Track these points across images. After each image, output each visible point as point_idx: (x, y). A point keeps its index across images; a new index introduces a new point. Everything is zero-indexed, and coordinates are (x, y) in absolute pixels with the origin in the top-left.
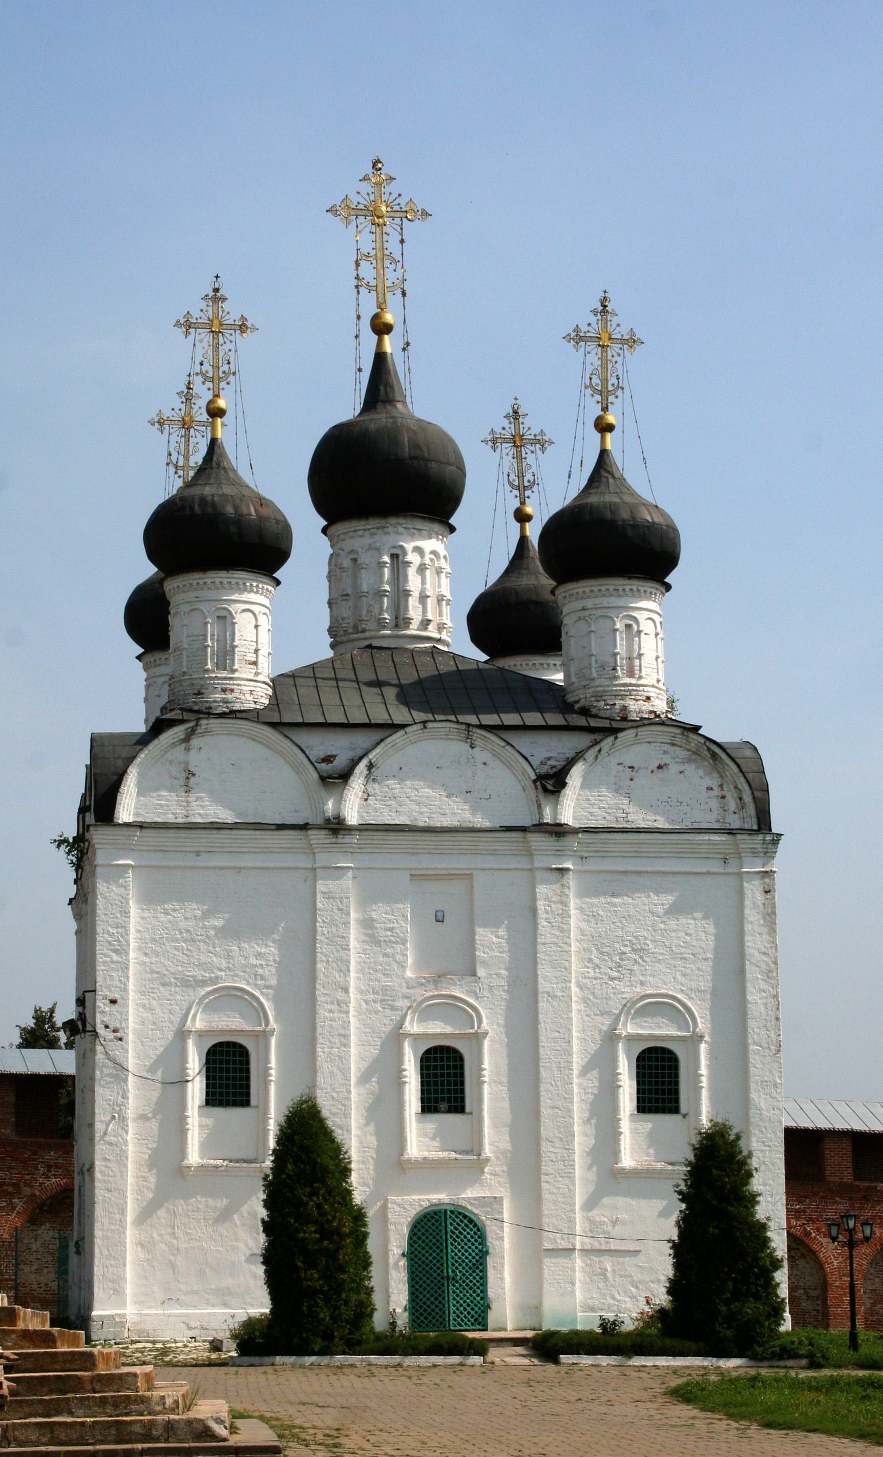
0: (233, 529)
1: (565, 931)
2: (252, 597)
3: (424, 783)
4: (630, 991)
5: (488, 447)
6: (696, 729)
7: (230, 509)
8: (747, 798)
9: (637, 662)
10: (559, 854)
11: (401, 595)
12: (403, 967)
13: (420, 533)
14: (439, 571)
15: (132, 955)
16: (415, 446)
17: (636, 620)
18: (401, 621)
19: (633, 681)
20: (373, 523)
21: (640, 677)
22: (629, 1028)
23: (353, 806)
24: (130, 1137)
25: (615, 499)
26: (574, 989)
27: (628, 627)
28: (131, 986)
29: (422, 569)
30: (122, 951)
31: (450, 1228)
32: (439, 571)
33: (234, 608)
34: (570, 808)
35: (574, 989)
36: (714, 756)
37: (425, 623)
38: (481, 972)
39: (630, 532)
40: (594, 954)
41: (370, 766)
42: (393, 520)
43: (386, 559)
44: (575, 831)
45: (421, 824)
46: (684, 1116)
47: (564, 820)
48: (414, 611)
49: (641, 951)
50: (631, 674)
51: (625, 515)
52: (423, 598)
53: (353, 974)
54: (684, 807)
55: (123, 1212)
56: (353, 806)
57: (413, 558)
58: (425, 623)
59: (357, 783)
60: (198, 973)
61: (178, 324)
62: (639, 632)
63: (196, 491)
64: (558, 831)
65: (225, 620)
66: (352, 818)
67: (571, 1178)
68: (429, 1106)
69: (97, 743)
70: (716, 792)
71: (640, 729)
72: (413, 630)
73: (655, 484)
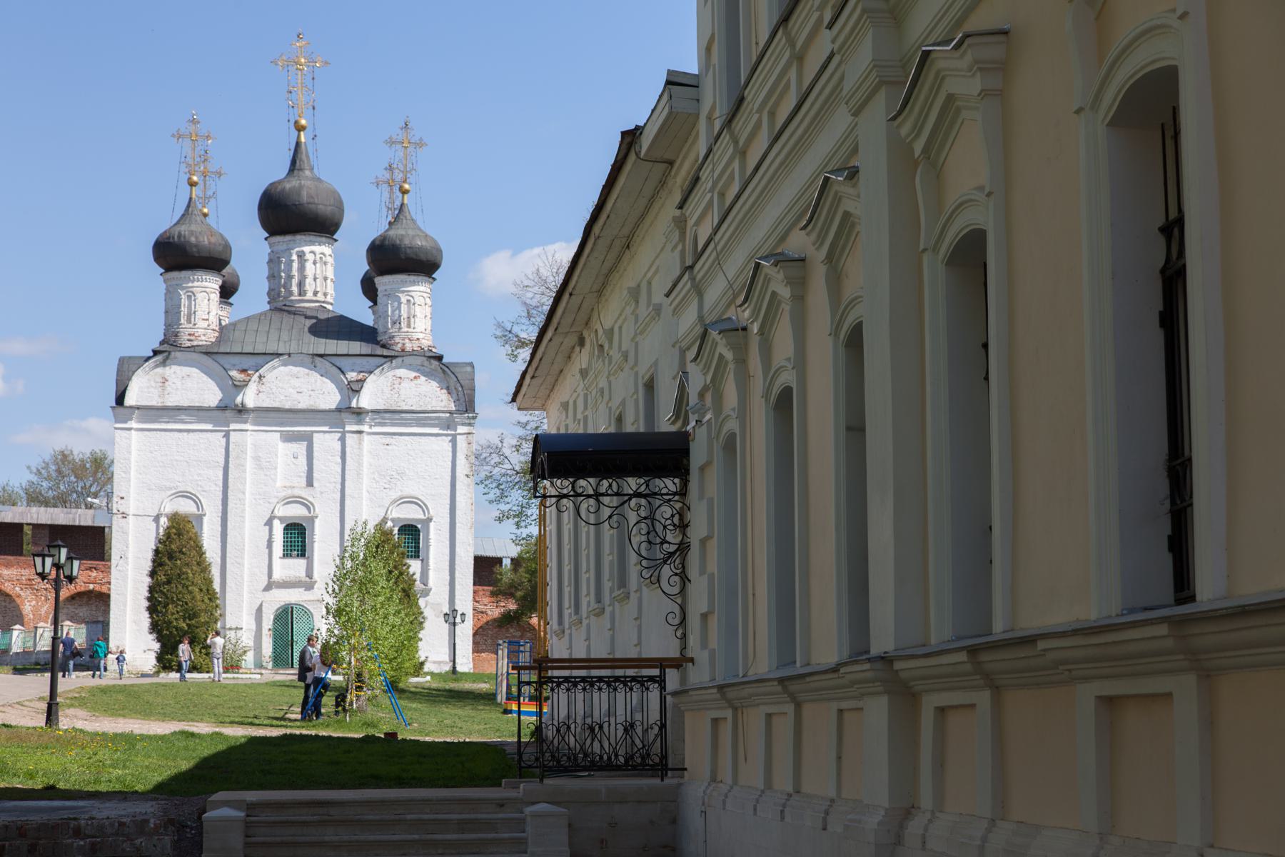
1: (360, 464)
3: (293, 384)
4: (395, 495)
5: (374, 187)
6: (440, 358)
7: (193, 239)
8: (461, 394)
10: (360, 422)
12: (275, 481)
13: (312, 243)
14: (325, 263)
15: (132, 473)
16: (310, 196)
18: (302, 292)
20: (288, 238)
23: (250, 397)
24: (130, 567)
25: (403, 232)
26: (365, 494)
28: (132, 490)
30: (127, 472)
32: (325, 263)
34: (366, 400)
35: (365, 494)
36: (444, 372)
37: (315, 293)
38: (315, 484)
40: (376, 476)
41: (260, 377)
42: (298, 237)
43: (295, 257)
44: (367, 412)
47: (361, 405)
48: (309, 286)
49: (401, 474)
50: (409, 326)
51: (407, 242)
52: (315, 279)
55: (125, 605)
57: (310, 257)
58: (315, 293)
60: (168, 484)
61: (173, 136)
63: (177, 229)
66: (250, 403)
68: (287, 555)
69: (122, 361)
72: (309, 296)
73: (429, 225)
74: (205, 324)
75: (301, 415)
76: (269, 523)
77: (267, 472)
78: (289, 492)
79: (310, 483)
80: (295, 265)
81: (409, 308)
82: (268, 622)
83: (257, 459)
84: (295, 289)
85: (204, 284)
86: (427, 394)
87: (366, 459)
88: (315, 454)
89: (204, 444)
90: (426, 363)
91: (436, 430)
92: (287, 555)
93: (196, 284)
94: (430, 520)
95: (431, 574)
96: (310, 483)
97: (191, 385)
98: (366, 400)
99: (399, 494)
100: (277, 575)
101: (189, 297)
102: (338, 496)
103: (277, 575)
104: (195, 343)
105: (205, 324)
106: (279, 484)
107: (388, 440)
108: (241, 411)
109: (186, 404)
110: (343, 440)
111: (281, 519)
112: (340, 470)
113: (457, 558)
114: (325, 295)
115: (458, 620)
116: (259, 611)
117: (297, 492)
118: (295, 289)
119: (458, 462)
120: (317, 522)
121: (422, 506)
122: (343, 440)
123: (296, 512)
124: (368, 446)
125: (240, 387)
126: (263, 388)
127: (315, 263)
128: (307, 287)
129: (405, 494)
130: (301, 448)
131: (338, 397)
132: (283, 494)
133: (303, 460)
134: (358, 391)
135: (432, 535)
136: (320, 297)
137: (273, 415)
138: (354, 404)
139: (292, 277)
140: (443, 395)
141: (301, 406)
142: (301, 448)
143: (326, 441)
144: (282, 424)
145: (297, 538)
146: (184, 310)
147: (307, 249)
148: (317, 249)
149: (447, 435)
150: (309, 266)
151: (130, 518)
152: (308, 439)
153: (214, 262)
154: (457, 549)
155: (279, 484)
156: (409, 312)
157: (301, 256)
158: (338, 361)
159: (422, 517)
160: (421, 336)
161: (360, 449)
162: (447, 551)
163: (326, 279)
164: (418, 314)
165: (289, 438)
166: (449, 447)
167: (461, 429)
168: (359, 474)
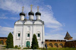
4: (37, 31)
22: (37, 33)
34: (35, 23)
49: (38, 29)
56: (25, 23)
64: (34, 24)
65: (22, 17)
68: (28, 36)
76: (26, 34)
77: (26, 30)
82: (26, 43)
83: (25, 28)
86: (40, 23)
87: (35, 28)
89: (21, 27)
92: (28, 36)
97: (21, 23)
98: (35, 23)
100: (27, 38)
103: (27, 38)
108: (24, 24)
116: (25, 42)
121: (40, 32)
123: (29, 33)
125: (24, 22)
130: (29, 28)
133: (29, 28)
142: (29, 28)
143: (31, 27)
145: (29, 35)
153: (24, 15)
165: (28, 27)
166: (42, 27)
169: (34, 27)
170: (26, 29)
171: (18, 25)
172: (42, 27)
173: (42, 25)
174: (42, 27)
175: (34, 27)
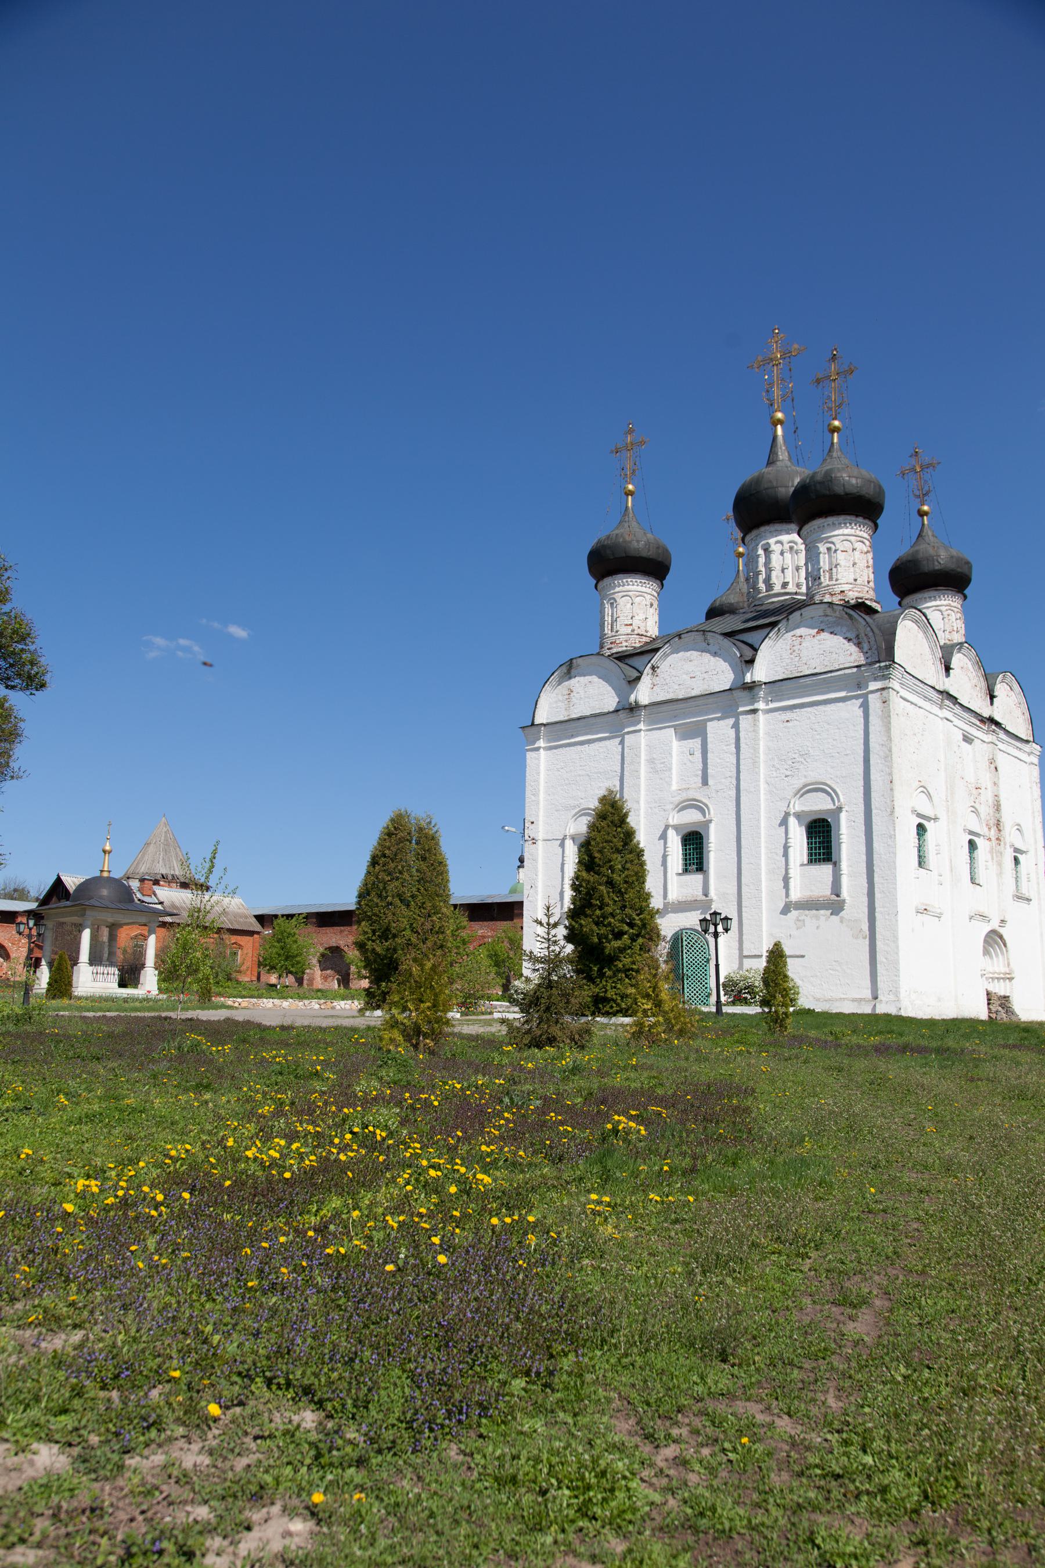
0: (608, 552)
1: (756, 750)
2: (630, 588)
4: (798, 783)
9: (834, 570)
11: (769, 570)
12: (670, 784)
13: (779, 533)
17: (833, 543)
18: (769, 586)
19: (834, 582)
21: (837, 580)
22: (798, 806)
26: (762, 786)
27: (829, 549)
28: (541, 813)
29: (782, 553)
31: (685, 943)
33: (617, 596)
34: (761, 671)
35: (762, 786)
37: (785, 585)
39: (818, 487)
41: (653, 668)
42: (762, 529)
43: (761, 552)
45: (681, 697)
46: (835, 864)
47: (756, 679)
48: (776, 579)
53: (643, 792)
54: (834, 655)
56: (644, 693)
57: (773, 547)
58: (785, 585)
59: (646, 680)
62: (836, 551)
66: (644, 700)
67: (761, 909)
70: (855, 641)
71: (803, 611)
72: (777, 589)
74: (629, 630)
75: (691, 703)
78: (685, 796)
79: (705, 782)
80: (762, 560)
81: (830, 557)
83: (651, 761)
84: (762, 586)
85: (627, 588)
88: (710, 746)
90: (829, 611)
91: (843, 694)
93: (617, 589)
94: (840, 809)
95: (845, 881)
96: (705, 782)
97: (593, 694)
99: (803, 781)
101: (612, 604)
102: (733, 793)
104: (614, 651)
105: (629, 630)
106: (674, 787)
107: (788, 715)
109: (588, 712)
110: (736, 726)
111: (676, 828)
112: (735, 762)
113: (875, 856)
114: (798, 585)
115: (720, 928)
117: (692, 794)
118: (762, 586)
119: (871, 729)
120: (712, 827)
122: (736, 726)
123: (691, 817)
124: (764, 725)
126: (657, 680)
127: (782, 553)
128: (774, 580)
129: (809, 780)
130: (696, 743)
131: (732, 676)
132: (678, 799)
133: (698, 755)
134: (751, 662)
135: (844, 829)
136: (791, 588)
137: (664, 708)
138: (748, 678)
139: (758, 573)
140: (853, 648)
141: (694, 693)
143: (719, 730)
144: (676, 717)
146: (608, 619)
147: (772, 541)
148: (785, 538)
149: (856, 697)
150: (775, 558)
151: (540, 843)
152: (699, 731)
154: (875, 845)
155: (674, 787)
156: (830, 563)
157: (767, 550)
158: (745, 637)
159: (831, 806)
160: (845, 587)
161: (756, 731)
162: (863, 849)
163: (798, 569)
164: (842, 563)
165: (685, 734)
166: (860, 712)
167: (873, 686)
168: (755, 763)
169: (745, 721)
170: (659, 768)
171: (567, 729)
172: (865, 707)
173: (854, 683)
174: (865, 707)
175: (745, 721)
